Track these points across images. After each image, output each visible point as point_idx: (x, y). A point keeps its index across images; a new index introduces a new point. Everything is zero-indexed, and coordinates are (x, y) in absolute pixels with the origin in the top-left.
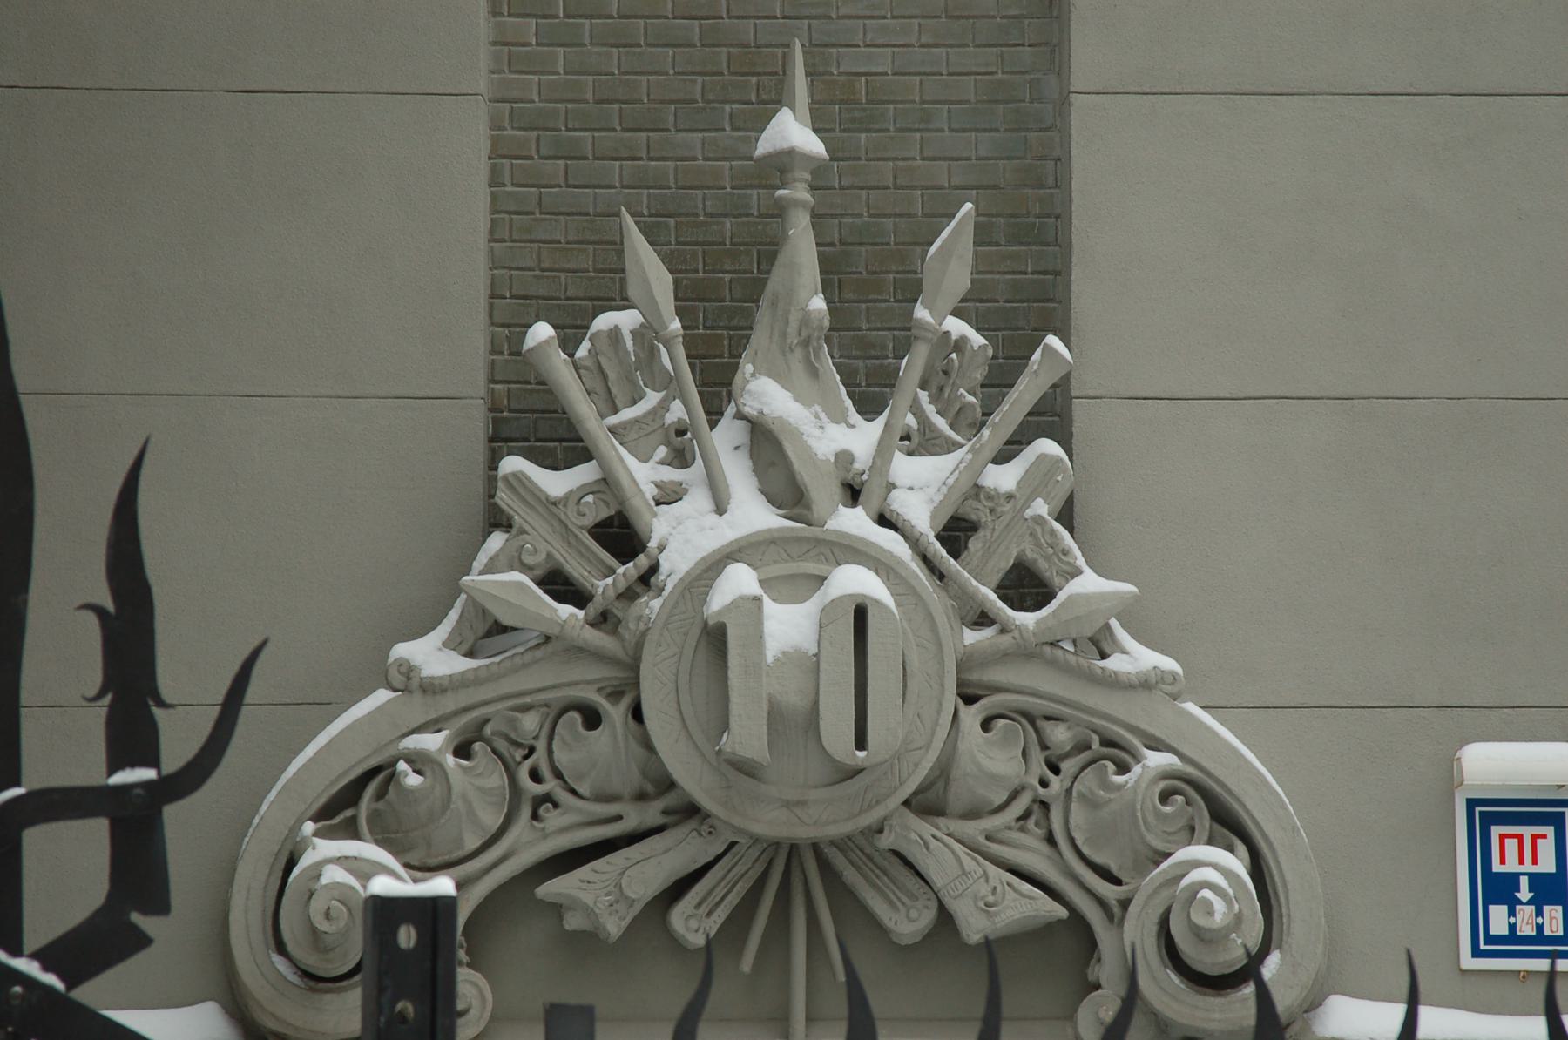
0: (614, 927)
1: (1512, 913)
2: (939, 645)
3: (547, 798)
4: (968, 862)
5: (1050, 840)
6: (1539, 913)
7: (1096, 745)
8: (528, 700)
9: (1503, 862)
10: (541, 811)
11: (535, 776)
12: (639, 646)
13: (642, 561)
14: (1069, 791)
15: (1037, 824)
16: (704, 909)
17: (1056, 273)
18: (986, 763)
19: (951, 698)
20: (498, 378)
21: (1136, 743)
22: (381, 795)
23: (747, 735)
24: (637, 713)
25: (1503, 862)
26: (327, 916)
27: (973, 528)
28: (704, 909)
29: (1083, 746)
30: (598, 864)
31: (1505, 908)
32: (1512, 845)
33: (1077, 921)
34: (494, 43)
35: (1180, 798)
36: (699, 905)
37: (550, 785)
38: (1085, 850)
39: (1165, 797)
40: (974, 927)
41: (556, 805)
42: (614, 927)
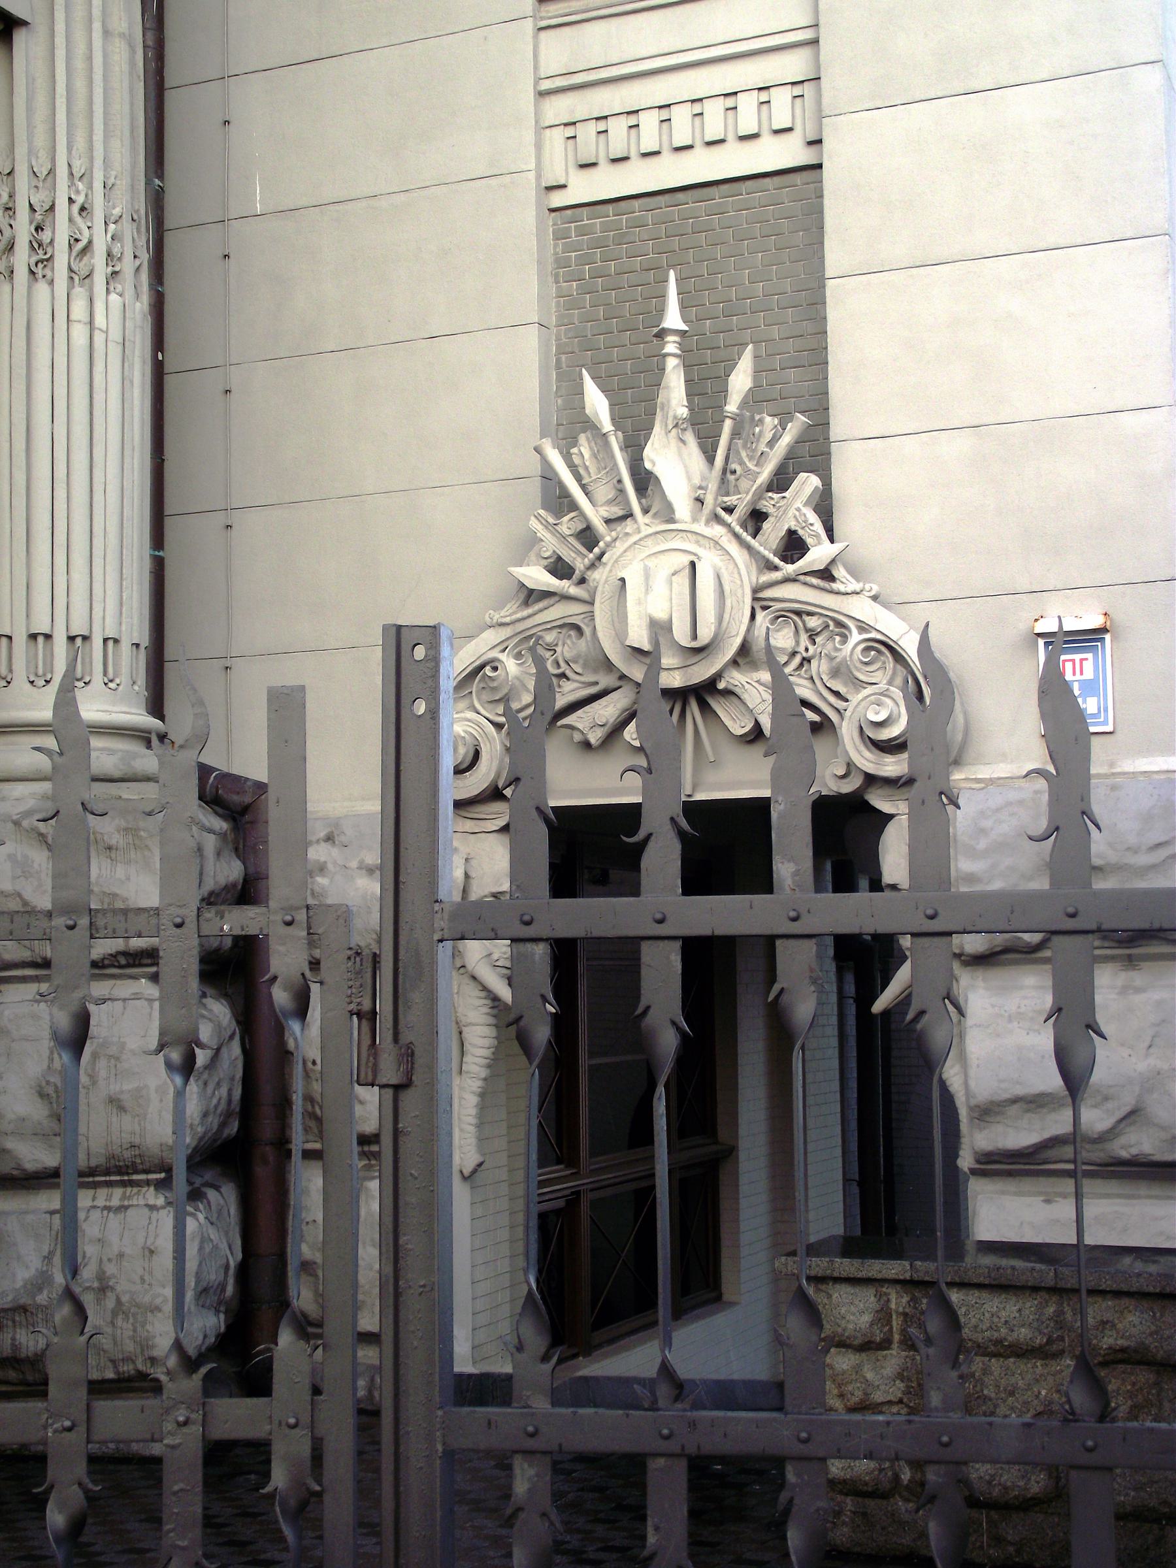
0: (594, 738)
3: (563, 676)
13: (596, 550)
23: (639, 636)
32: (1069, 666)
35: (873, 653)
41: (568, 679)
42: (594, 738)
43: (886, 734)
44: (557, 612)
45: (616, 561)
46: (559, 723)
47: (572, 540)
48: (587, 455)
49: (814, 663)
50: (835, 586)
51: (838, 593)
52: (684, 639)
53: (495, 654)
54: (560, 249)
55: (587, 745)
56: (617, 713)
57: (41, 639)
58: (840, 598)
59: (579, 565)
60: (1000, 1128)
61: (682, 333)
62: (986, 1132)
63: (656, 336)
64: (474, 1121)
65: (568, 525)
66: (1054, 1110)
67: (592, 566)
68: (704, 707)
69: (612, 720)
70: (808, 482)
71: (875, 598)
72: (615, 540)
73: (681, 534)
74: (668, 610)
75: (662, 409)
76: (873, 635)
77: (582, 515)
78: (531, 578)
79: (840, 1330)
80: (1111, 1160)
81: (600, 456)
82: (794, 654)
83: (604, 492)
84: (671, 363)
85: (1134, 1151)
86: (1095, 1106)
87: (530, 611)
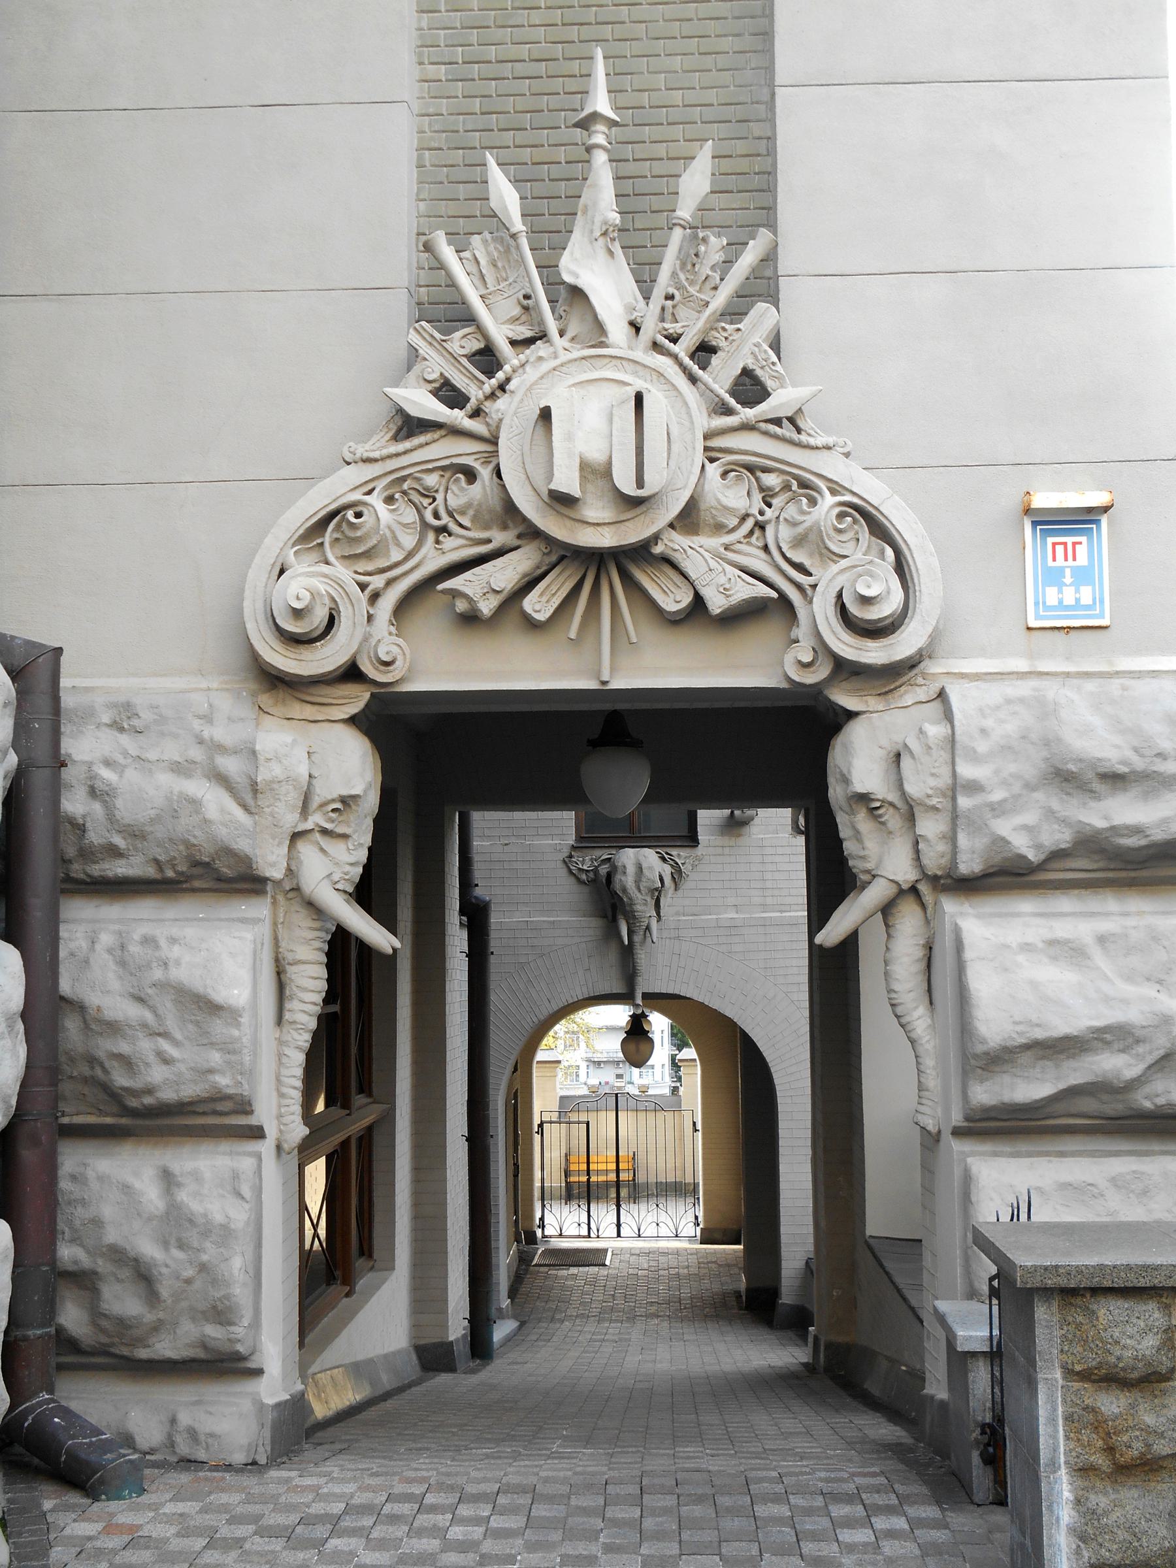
0: (487, 607)
1: (1060, 591)
2: (692, 423)
3: (444, 530)
4: (713, 564)
5: (766, 548)
6: (1077, 591)
7: (795, 487)
8: (430, 466)
9: (1054, 559)
10: (441, 538)
11: (436, 516)
12: (498, 427)
13: (500, 375)
14: (778, 518)
15: (757, 539)
16: (544, 599)
17: (769, 209)
18: (725, 501)
20: (422, 283)
21: (822, 485)
22: (338, 527)
23: (567, 481)
24: (498, 474)
25: (1054, 559)
26: (298, 598)
27: (713, 350)
28: (544, 599)
29: (787, 487)
31: (1055, 589)
32: (1060, 549)
33: (783, 598)
34: (419, 81)
35: (849, 519)
36: (541, 595)
37: (445, 519)
39: (841, 516)
40: (716, 603)
42: (487, 607)
43: (873, 614)
45: (529, 389)
46: (440, 587)
47: (464, 361)
48: (483, 262)
49: (770, 531)
50: (803, 438)
52: (628, 486)
53: (357, 496)
54: (424, 24)
55: (470, 619)
56: (518, 577)
58: (807, 452)
59: (475, 394)
60: (1006, 1079)
61: (613, 124)
62: (988, 1083)
63: (576, 125)
65: (463, 342)
66: (1073, 1056)
67: (492, 396)
69: (509, 587)
70: (762, 316)
71: (847, 455)
72: (523, 365)
73: (614, 362)
74: (608, 453)
75: (585, 212)
76: (848, 498)
77: (481, 330)
78: (415, 402)
80: (1128, 1113)
81: (500, 264)
82: (744, 518)
85: (1161, 1101)
86: (1123, 1051)
87: (407, 444)
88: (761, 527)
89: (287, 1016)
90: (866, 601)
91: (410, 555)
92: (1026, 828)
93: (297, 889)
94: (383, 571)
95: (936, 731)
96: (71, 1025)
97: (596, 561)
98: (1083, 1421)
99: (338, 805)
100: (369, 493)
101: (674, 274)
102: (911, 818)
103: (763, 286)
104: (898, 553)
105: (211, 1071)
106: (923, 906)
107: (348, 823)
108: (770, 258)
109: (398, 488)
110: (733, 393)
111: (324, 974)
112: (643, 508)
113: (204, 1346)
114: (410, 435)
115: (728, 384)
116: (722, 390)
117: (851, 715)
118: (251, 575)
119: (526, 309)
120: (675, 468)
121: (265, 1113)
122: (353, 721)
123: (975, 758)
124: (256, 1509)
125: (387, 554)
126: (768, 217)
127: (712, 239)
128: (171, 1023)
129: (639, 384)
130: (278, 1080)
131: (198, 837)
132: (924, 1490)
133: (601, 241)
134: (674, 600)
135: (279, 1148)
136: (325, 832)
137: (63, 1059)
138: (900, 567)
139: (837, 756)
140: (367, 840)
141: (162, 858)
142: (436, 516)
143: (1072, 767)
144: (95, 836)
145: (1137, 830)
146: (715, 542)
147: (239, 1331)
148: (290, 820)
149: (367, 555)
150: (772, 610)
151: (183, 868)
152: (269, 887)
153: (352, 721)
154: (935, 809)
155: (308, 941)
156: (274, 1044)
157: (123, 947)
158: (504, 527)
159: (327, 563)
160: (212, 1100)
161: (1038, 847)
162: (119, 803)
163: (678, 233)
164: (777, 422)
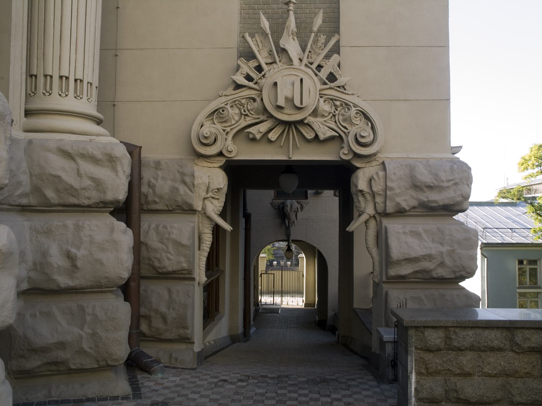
0: (258, 136)
3: (247, 115)
5: (335, 122)
11: (245, 111)
12: (262, 88)
13: (263, 73)
19: (318, 96)
21: (351, 104)
23: (281, 102)
24: (262, 100)
27: (322, 67)
29: (342, 105)
30: (256, 126)
33: (340, 137)
38: (342, 124)
39: (357, 113)
40: (322, 137)
44: (246, 93)
46: (246, 131)
47: (253, 69)
49: (337, 117)
50: (346, 92)
51: (348, 94)
53: (223, 105)
55: (254, 140)
57: (64, 78)
61: (294, 4)
64: (204, 266)
65: (253, 64)
68: (297, 129)
71: (358, 97)
76: (359, 108)
79: (428, 345)
82: (330, 113)
83: (265, 53)
84: (291, 13)
85: (440, 275)
87: (237, 91)
88: (334, 116)
89: (202, 248)
90: (363, 137)
91: (237, 122)
92: (405, 200)
93: (205, 213)
94: (229, 126)
95: (381, 173)
96: (143, 249)
97: (288, 124)
98: (420, 361)
99: (216, 190)
100: (226, 104)
101: (311, 46)
102: (374, 197)
103: (336, 49)
104: (372, 124)
105: (182, 263)
106: (376, 221)
107: (219, 195)
108: (338, 42)
109: (235, 104)
110: (327, 79)
111: (211, 236)
112: (302, 110)
113: (179, 335)
114: (237, 89)
115: (326, 76)
116: (324, 78)
117: (358, 168)
118: (194, 127)
119: (270, 54)
120: (310, 100)
121: (196, 275)
122: (220, 167)
123: (392, 181)
124: (195, 380)
125: (231, 122)
126: (336, 30)
127: (322, 36)
128: (171, 249)
129: (302, 76)
130: (199, 265)
131: (179, 199)
132: (372, 377)
133: (291, 36)
134: (310, 135)
135: (199, 284)
136: (213, 198)
137: (141, 258)
138: (373, 128)
139: (353, 179)
140: (224, 200)
141: (168, 204)
142: (245, 111)
143: (418, 184)
144: (150, 198)
145: (436, 202)
146: (322, 120)
147: (189, 332)
148: (203, 194)
149: (225, 122)
150: (338, 139)
151: (173, 207)
152: (197, 213)
153: (220, 167)
154: (380, 194)
155: (207, 228)
156: (198, 255)
157: (157, 229)
158: (263, 114)
159: (214, 124)
160: (182, 270)
161: (408, 205)
162: (157, 189)
163: (313, 34)
164: (339, 87)
